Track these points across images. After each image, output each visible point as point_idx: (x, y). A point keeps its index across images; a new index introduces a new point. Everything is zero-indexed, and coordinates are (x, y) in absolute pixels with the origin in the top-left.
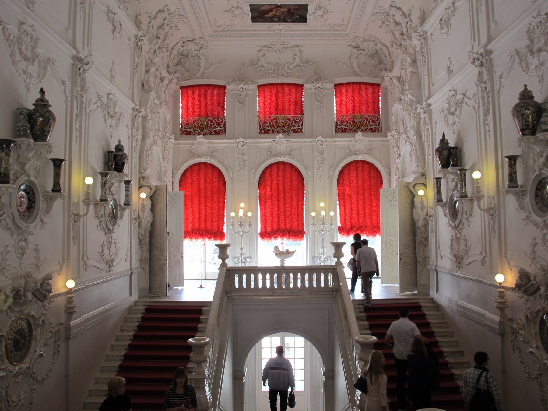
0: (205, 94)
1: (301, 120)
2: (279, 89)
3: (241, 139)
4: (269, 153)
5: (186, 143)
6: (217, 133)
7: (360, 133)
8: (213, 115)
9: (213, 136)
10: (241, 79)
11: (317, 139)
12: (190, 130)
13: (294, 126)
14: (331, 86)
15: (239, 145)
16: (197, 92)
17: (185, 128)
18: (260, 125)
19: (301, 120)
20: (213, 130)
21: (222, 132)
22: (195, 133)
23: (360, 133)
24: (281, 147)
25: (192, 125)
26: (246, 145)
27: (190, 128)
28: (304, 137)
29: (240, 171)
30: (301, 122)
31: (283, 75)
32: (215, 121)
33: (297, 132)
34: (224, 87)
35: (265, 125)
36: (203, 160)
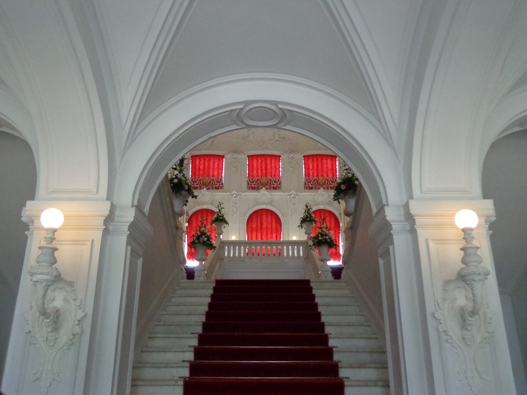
0: (209, 161)
1: (279, 181)
3: (234, 192)
6: (217, 188)
7: (322, 189)
8: (213, 176)
9: (214, 190)
10: (236, 151)
11: (290, 193)
14: (301, 157)
16: (202, 161)
18: (249, 184)
19: (279, 181)
22: (200, 188)
23: (322, 189)
24: (264, 198)
26: (238, 197)
33: (276, 189)
34: (223, 157)
36: (205, 207)
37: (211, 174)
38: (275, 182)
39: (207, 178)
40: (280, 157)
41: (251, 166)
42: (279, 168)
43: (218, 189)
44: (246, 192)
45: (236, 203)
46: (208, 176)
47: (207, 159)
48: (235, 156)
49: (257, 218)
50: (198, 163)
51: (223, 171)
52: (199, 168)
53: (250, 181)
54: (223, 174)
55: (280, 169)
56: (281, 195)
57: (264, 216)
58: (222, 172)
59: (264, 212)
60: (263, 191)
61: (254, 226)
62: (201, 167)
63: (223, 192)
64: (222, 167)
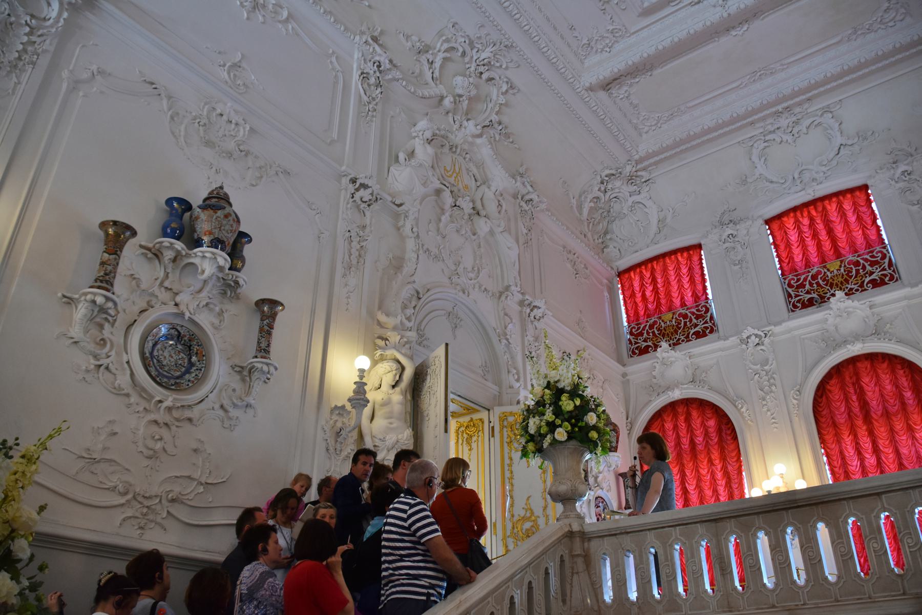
2: (814, 213)
4: (823, 345)
5: (641, 367)
6: (698, 335)
12: (646, 344)
13: (871, 273)
15: (751, 345)
17: (636, 343)
20: (692, 331)
21: (711, 332)
22: (656, 347)
25: (648, 333)
26: (767, 341)
27: (645, 341)
28: (904, 286)
29: (764, 399)
30: (887, 261)
31: (814, 180)
32: (693, 313)
34: (699, 247)
35: (802, 292)
36: (676, 395)
37: (677, 302)
38: (872, 264)
39: (668, 316)
40: (866, 187)
41: (782, 246)
42: (875, 219)
43: (705, 335)
44: (789, 319)
45: (766, 362)
46: (670, 309)
47: (658, 267)
48: (730, 232)
49: (843, 388)
50: (636, 284)
51: (708, 284)
52: (644, 296)
53: (790, 285)
54: (709, 291)
55: (879, 222)
56: (906, 298)
57: (866, 380)
58: (705, 288)
59: (863, 366)
60: (839, 300)
61: (841, 419)
62: (648, 293)
63: (719, 338)
64: (703, 275)
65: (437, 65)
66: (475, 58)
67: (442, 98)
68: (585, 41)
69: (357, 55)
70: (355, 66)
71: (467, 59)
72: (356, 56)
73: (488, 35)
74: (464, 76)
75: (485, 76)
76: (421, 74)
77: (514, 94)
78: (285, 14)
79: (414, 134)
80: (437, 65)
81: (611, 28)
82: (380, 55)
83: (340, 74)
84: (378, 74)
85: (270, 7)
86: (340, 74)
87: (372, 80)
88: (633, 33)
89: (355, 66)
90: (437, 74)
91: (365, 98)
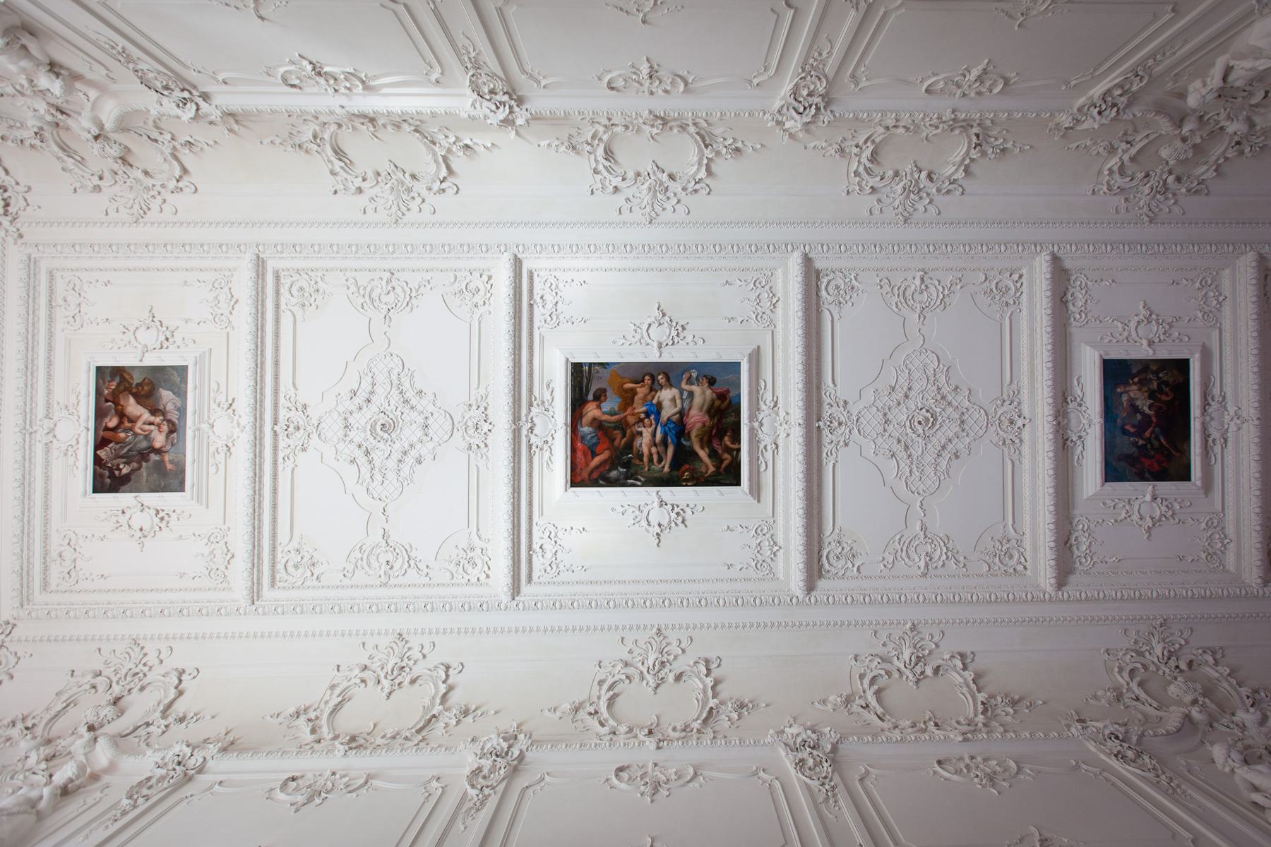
65: (1143, 696)
66: (1156, 660)
67: (1187, 717)
68: (1203, 556)
69: (1091, 747)
70: (1103, 757)
71: (1152, 668)
72: (1093, 749)
73: (1138, 632)
74: (1170, 683)
75: (1183, 666)
76: (1146, 716)
77: (1223, 656)
78: (1012, 764)
79: (1227, 770)
80: (1143, 696)
81: (1203, 525)
82: (1105, 727)
83: (1106, 774)
84: (1126, 745)
85: (998, 768)
86: (1106, 774)
87: (1130, 754)
88: (1223, 509)
89: (1103, 757)
90: (1155, 704)
91: (1150, 775)
